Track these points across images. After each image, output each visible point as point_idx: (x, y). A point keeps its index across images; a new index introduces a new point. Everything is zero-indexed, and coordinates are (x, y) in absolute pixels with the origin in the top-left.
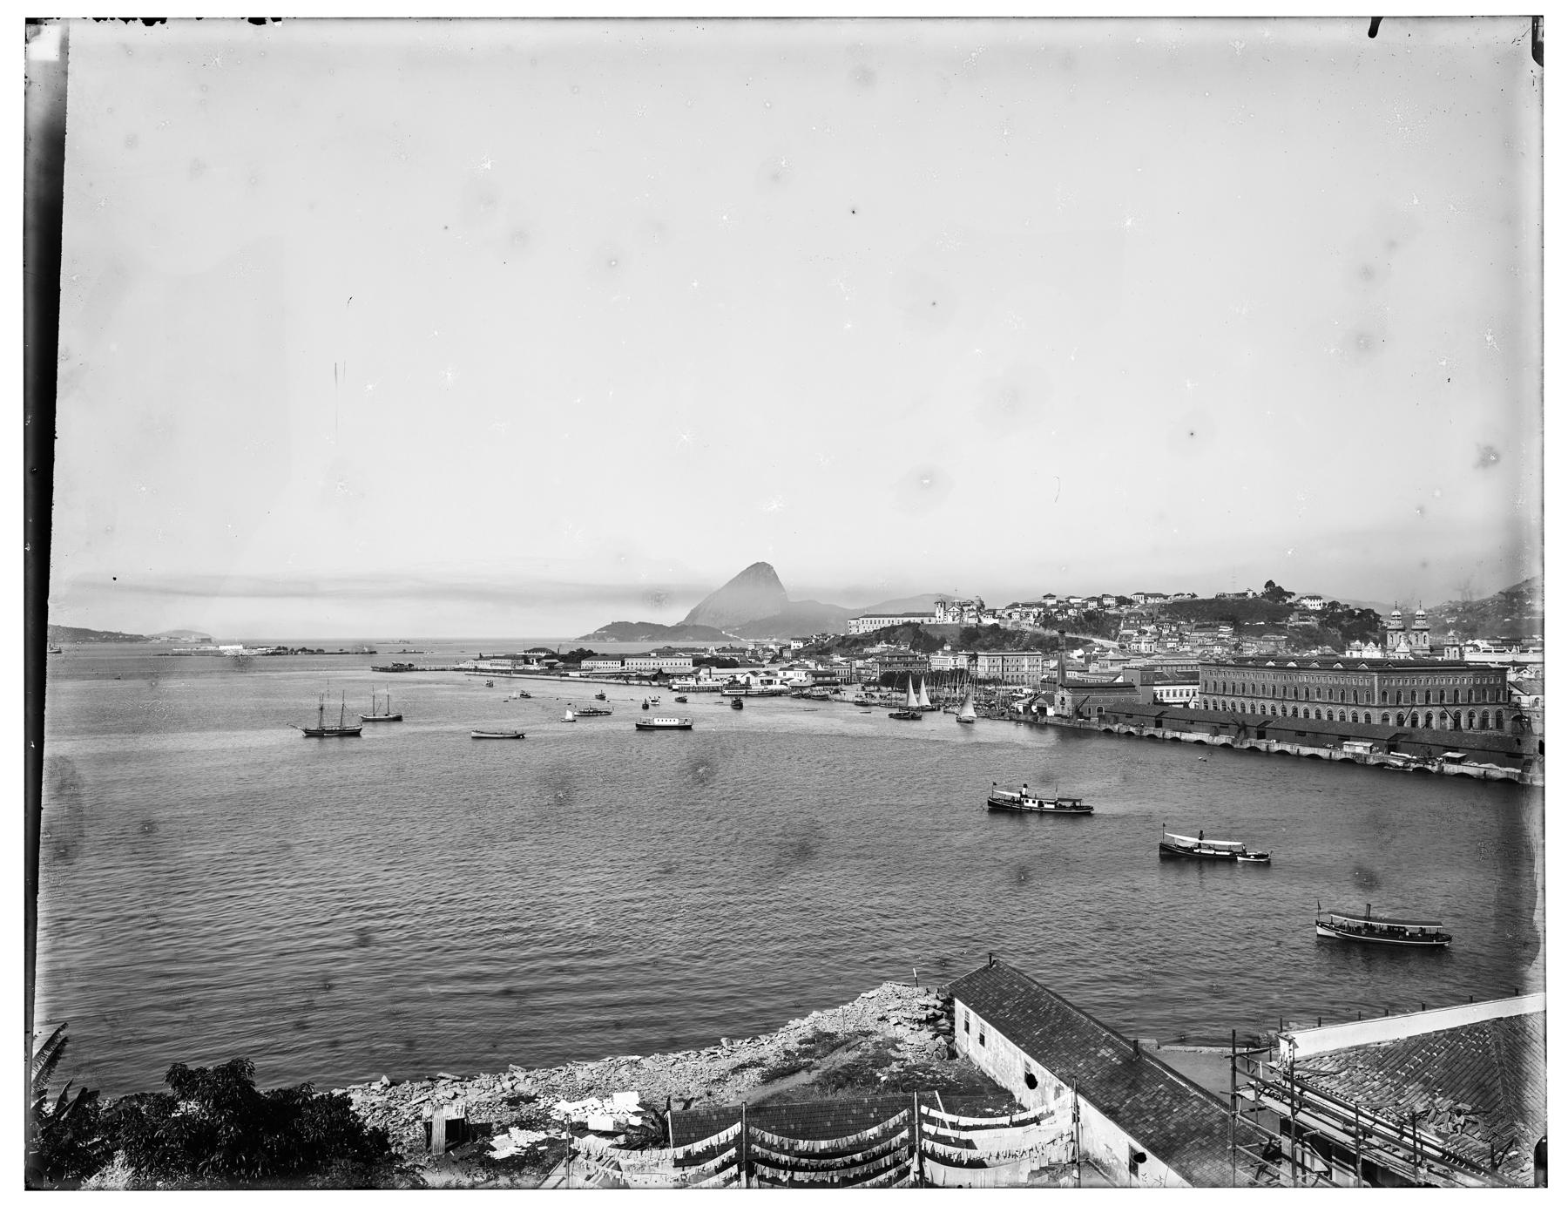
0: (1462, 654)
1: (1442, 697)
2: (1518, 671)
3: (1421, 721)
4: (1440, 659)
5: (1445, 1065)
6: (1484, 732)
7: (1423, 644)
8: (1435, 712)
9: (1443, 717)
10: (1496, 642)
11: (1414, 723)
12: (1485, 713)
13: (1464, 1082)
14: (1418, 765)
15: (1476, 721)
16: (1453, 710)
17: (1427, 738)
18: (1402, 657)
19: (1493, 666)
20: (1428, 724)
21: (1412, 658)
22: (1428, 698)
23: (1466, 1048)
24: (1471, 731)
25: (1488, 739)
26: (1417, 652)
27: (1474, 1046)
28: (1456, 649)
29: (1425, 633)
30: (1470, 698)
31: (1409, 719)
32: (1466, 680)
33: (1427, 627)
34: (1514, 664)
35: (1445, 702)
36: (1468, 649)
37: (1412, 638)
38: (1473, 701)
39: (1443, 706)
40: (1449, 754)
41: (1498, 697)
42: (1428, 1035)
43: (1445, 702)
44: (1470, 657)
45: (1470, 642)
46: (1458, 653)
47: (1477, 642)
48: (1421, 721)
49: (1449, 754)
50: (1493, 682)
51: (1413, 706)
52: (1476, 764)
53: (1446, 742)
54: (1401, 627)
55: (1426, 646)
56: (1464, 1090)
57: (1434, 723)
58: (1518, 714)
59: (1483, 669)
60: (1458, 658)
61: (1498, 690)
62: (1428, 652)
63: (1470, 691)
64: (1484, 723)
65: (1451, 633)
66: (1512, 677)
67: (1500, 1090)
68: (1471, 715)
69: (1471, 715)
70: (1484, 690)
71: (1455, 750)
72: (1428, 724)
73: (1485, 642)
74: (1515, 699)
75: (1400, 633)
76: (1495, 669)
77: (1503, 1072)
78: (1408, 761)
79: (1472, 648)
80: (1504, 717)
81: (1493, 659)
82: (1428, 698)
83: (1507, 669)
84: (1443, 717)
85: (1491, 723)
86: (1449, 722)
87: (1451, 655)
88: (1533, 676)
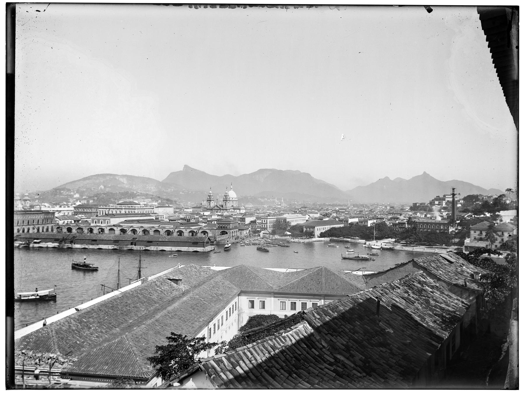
0: (40, 208)
1: (33, 222)
2: (59, 213)
3: (26, 231)
4: (33, 210)
5: (35, 342)
6: (47, 233)
7: (28, 204)
8: (31, 227)
9: (34, 229)
10: (52, 204)
11: (23, 231)
12: (48, 227)
13: (41, 346)
14: (24, 246)
15: (45, 230)
16: (37, 226)
17: (28, 236)
18: (20, 209)
19: (50, 212)
20: (28, 231)
21: (23, 210)
22: (28, 222)
23: (42, 335)
24: (43, 233)
25: (48, 235)
26: (25, 208)
27: (44, 333)
28: (38, 206)
29: (28, 201)
30: (43, 222)
31: (22, 230)
32: (42, 216)
33: (28, 199)
34: (57, 211)
35: (34, 224)
36: (42, 206)
37: (23, 202)
38: (44, 223)
39: (33, 225)
40: (35, 241)
41: (52, 221)
42: (29, 334)
43: (34, 224)
44: (43, 209)
45: (43, 204)
46: (39, 208)
47: (46, 204)
48: (26, 231)
49: (35, 241)
50: (50, 217)
51: (23, 226)
52: (44, 243)
53: (35, 237)
54: (19, 199)
55: (28, 205)
56: (41, 348)
57: (31, 231)
58: (58, 226)
59: (47, 213)
60: (39, 209)
61: (52, 219)
62: (29, 208)
63: (43, 220)
64: (47, 230)
65: (37, 201)
66: (56, 215)
67: (53, 345)
68: (43, 228)
69: (43, 228)
70: (48, 220)
71: (37, 239)
72: (28, 231)
73: (48, 204)
74: (57, 222)
75: (19, 201)
76: (51, 213)
77: (53, 339)
78: (22, 244)
79: (44, 206)
80: (54, 228)
81: (51, 209)
82: (28, 222)
83: (54, 213)
84: (34, 229)
85: (50, 230)
86: (36, 231)
87: (37, 208)
88: (63, 215)
